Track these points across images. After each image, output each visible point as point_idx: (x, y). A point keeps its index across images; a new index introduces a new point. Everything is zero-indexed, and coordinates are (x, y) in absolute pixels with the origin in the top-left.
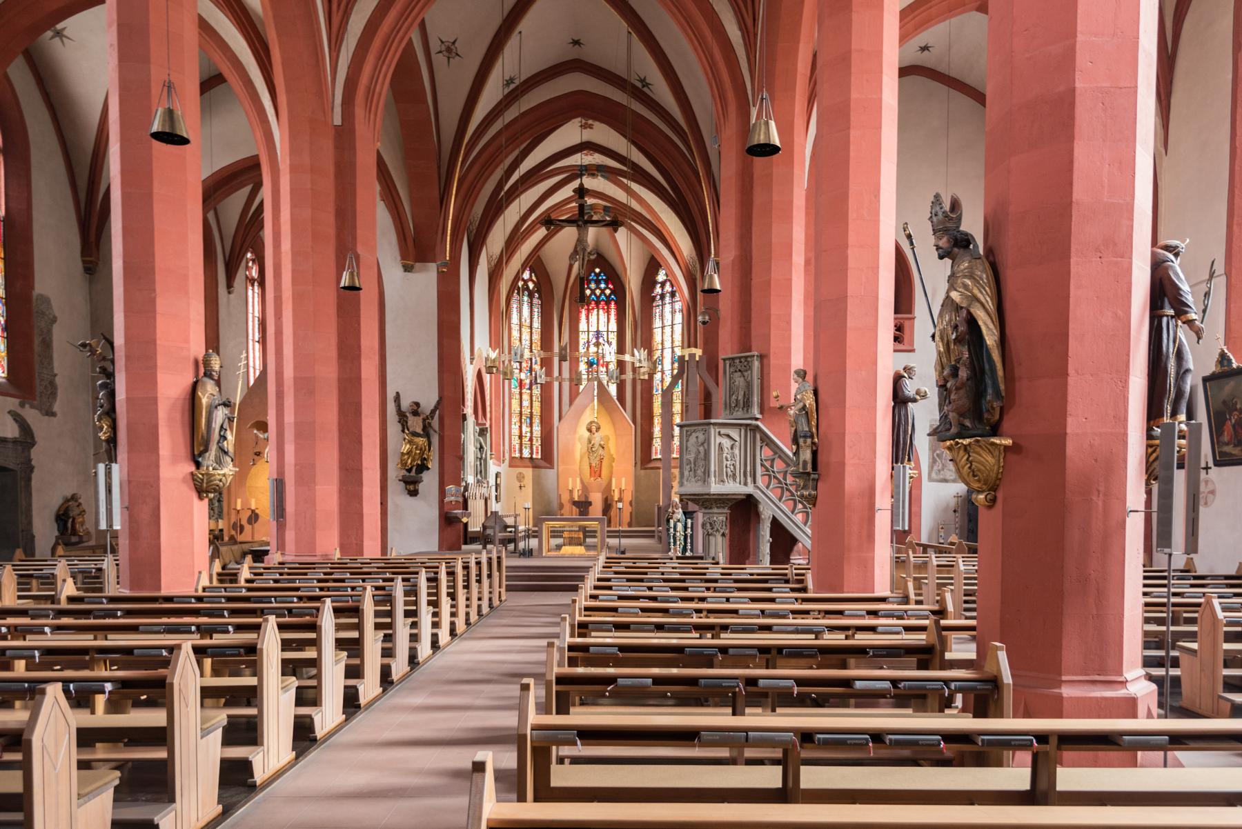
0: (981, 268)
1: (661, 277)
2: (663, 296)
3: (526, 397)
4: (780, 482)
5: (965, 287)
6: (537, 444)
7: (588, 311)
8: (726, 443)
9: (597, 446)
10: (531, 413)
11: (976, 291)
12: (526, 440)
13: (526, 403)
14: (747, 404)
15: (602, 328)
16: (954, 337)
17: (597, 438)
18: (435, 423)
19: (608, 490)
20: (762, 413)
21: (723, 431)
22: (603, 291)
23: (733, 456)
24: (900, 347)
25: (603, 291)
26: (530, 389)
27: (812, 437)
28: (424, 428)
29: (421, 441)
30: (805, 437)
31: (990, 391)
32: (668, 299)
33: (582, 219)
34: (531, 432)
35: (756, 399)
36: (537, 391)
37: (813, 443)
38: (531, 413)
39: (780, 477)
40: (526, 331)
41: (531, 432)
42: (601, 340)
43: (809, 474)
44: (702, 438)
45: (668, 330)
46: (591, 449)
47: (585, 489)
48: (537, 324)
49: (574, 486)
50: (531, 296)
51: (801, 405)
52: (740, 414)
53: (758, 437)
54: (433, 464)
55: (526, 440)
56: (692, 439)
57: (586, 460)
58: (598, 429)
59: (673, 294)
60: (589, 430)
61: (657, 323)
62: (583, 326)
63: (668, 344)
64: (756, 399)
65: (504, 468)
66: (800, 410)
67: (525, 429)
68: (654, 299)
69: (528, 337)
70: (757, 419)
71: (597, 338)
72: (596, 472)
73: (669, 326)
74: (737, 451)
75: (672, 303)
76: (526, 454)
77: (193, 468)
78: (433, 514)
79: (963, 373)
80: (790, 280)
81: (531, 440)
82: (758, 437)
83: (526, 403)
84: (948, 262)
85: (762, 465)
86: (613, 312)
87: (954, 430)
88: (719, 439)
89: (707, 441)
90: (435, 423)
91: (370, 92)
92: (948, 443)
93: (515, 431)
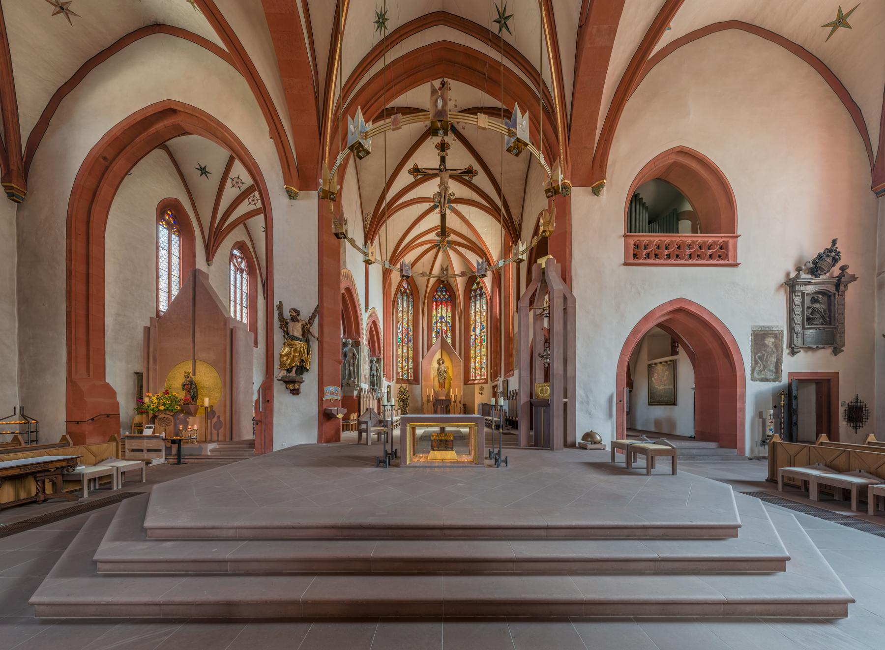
2: (475, 297)
3: (405, 348)
6: (411, 372)
12: (405, 370)
13: (405, 351)
15: (444, 314)
17: (443, 367)
19: (448, 394)
22: (444, 296)
25: (444, 296)
36: (411, 345)
47: (436, 394)
48: (410, 311)
49: (430, 392)
55: (405, 370)
57: (437, 379)
58: (443, 362)
59: (481, 295)
60: (439, 363)
61: (472, 311)
62: (434, 314)
63: (478, 320)
65: (393, 384)
67: (405, 364)
68: (470, 298)
72: (442, 385)
76: (405, 377)
83: (405, 351)
93: (400, 365)
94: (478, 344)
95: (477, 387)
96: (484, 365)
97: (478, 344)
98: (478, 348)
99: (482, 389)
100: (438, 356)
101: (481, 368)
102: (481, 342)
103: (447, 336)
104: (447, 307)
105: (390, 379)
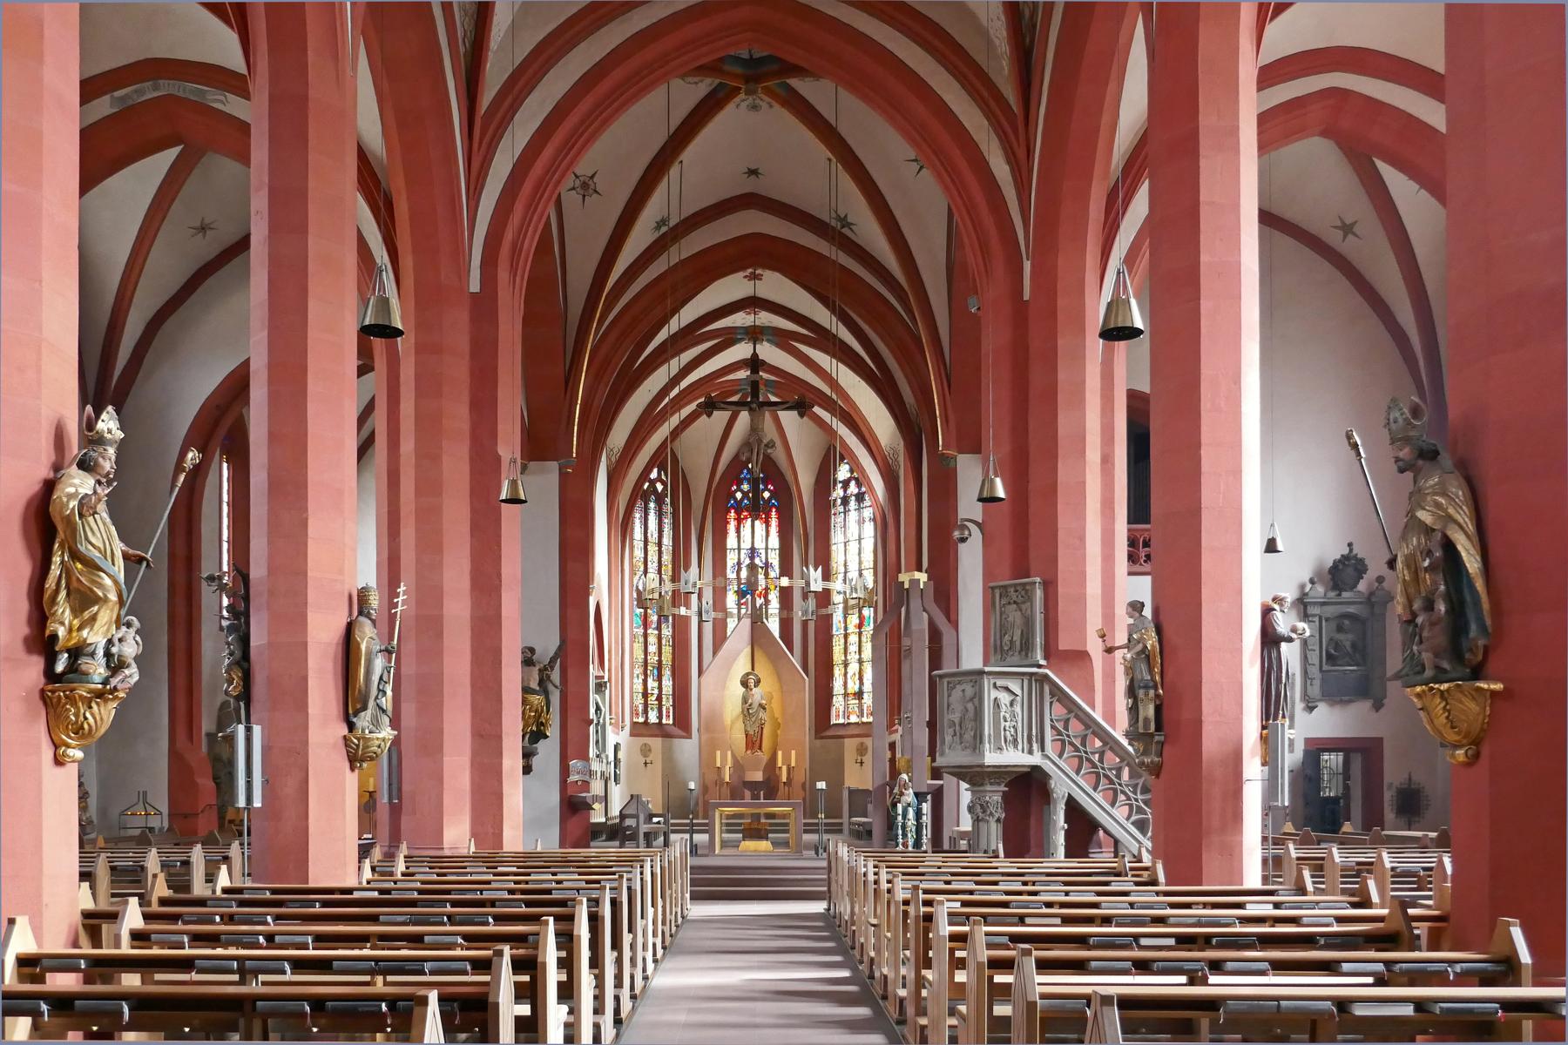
0: (1455, 483)
1: (843, 472)
2: (845, 501)
3: (652, 640)
4: (1077, 750)
5: (1438, 505)
6: (668, 703)
7: (739, 521)
8: (1005, 698)
9: (755, 706)
10: (660, 661)
11: (1451, 511)
12: (652, 699)
13: (652, 649)
14: (1026, 647)
15: (759, 544)
16: (1426, 563)
17: (757, 693)
18: (556, 675)
20: (1046, 657)
21: (999, 683)
23: (1014, 716)
24: (1137, 568)
26: (659, 628)
27: (1156, 688)
28: (541, 683)
29: (536, 699)
30: (1146, 687)
31: (1473, 627)
32: (853, 504)
33: (753, 399)
34: (660, 688)
35: (1039, 640)
36: (667, 632)
37: (1157, 696)
38: (660, 661)
39: (1077, 742)
40: (653, 549)
41: (660, 688)
42: (757, 561)
43: (1152, 735)
44: (969, 691)
45: (853, 547)
46: (747, 710)
47: (738, 766)
48: (667, 540)
49: (725, 763)
50: (660, 502)
51: (1140, 647)
52: (1016, 659)
53: (1047, 689)
54: (553, 731)
55: (652, 699)
56: (957, 693)
57: (740, 726)
58: (757, 683)
59: (860, 498)
60: (744, 683)
62: (731, 541)
64: (1039, 640)
66: (1138, 654)
67: (652, 684)
69: (656, 559)
70: (1040, 666)
71: (752, 558)
72: (753, 742)
73: (855, 542)
74: (1018, 709)
75: (859, 509)
77: (345, 731)
78: (554, 798)
79: (1441, 607)
80: (1084, 483)
81: (659, 698)
82: (1047, 689)
83: (652, 649)
84: (1409, 475)
85: (1053, 727)
86: (774, 522)
87: (1429, 673)
88: (994, 694)
89: (978, 697)
90: (556, 675)
91: (516, 250)
92: (1418, 689)
93: (639, 687)
94: (852, 629)
95: (850, 745)
96: (868, 687)
97: (852, 629)
98: (853, 639)
99: (862, 750)
100: (742, 666)
101: (859, 695)
102: (860, 626)
103: (767, 602)
104: (768, 525)
105: (619, 727)
